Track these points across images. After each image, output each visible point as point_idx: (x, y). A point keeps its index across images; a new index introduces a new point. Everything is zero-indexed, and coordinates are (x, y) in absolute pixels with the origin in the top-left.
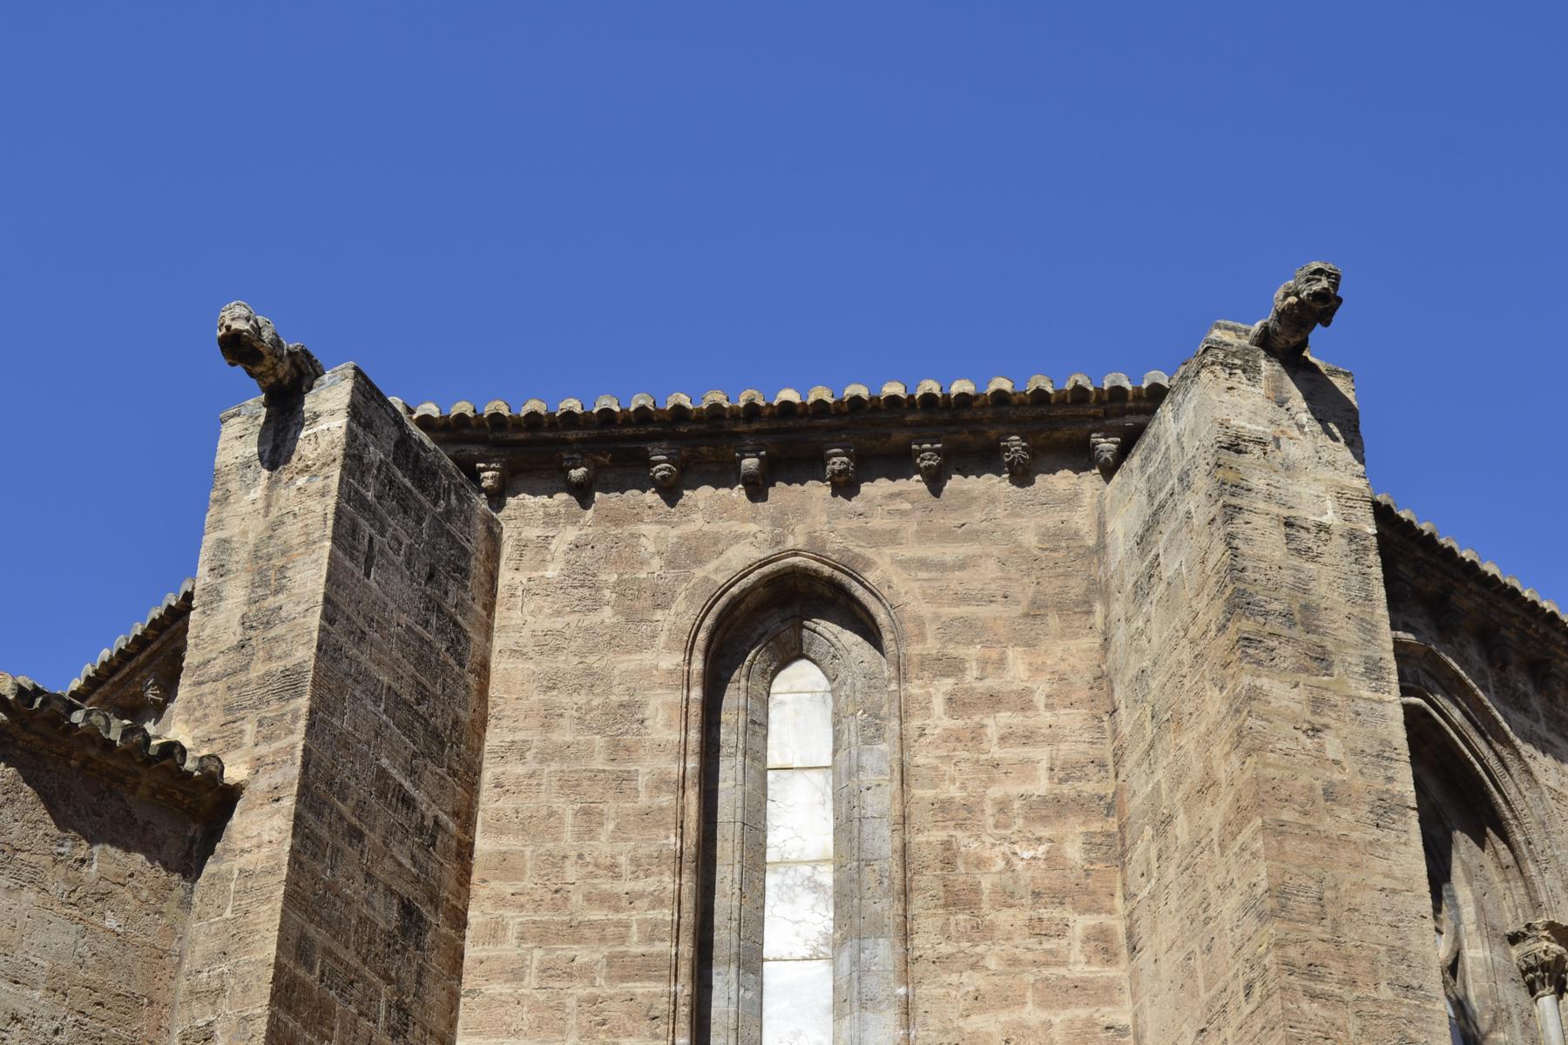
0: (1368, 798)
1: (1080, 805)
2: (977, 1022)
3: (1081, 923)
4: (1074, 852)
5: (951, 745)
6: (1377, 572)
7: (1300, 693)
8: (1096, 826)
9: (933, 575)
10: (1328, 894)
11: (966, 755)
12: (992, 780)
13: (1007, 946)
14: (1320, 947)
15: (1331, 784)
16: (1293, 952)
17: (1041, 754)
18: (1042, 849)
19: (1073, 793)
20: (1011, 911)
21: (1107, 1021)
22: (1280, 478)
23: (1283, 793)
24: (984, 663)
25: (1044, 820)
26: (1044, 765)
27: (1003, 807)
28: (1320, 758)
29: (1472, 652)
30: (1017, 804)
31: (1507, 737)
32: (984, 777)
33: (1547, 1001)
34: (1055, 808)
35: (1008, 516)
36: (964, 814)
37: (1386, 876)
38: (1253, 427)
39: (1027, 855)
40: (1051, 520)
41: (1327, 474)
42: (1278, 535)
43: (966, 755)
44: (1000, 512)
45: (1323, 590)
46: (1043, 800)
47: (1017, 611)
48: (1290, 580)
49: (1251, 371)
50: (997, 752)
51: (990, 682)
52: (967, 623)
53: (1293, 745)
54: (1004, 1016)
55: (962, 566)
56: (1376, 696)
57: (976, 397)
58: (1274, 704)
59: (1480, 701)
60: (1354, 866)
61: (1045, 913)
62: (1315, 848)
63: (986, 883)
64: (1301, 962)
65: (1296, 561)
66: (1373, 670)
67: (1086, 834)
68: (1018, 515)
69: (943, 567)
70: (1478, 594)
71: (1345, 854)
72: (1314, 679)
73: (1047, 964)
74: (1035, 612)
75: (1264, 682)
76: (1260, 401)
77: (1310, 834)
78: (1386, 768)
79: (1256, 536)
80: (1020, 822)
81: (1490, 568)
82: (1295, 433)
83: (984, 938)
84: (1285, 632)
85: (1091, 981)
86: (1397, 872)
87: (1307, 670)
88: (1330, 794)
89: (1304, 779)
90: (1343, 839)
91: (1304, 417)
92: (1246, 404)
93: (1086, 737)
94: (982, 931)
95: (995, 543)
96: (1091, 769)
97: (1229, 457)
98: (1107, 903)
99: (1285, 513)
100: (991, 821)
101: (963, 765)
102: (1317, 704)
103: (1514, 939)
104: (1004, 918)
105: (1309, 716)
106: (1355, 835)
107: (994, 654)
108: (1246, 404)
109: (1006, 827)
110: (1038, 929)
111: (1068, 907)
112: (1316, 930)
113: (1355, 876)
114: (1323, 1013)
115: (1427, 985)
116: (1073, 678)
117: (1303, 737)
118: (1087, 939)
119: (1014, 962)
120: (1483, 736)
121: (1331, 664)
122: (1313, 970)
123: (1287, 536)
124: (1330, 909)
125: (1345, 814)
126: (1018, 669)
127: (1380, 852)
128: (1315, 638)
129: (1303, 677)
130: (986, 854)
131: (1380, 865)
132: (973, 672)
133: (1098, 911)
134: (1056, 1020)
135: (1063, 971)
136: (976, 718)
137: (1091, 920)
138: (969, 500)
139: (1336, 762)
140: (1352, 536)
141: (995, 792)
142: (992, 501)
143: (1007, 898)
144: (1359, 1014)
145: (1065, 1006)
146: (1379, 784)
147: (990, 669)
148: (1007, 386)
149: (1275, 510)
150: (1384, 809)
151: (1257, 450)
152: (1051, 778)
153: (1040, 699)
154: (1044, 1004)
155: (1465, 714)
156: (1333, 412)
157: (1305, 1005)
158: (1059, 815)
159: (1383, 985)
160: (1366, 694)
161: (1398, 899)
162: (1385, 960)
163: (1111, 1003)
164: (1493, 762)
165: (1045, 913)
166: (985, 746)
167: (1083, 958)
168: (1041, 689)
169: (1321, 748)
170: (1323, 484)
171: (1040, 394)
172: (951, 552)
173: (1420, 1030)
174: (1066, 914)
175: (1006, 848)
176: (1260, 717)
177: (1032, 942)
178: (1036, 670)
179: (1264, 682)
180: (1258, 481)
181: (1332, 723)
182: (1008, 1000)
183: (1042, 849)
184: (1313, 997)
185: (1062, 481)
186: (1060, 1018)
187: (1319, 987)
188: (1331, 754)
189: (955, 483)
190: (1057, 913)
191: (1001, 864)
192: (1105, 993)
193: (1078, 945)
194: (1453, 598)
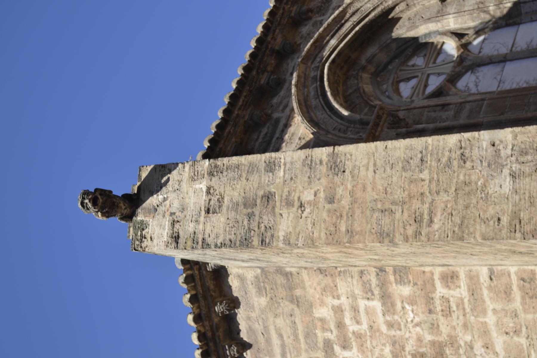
0: (331, 176)
1: (383, 285)
2: (499, 347)
3: (440, 290)
4: (406, 290)
5: (365, 350)
6: (226, 160)
7: (284, 212)
8: (392, 278)
9: (287, 351)
10: (379, 206)
11: (369, 342)
12: (379, 330)
13: (459, 329)
14: (406, 214)
15: (326, 198)
16: (410, 231)
17: (362, 304)
18: (408, 307)
19: (378, 289)
20: (441, 326)
21: (488, 279)
22: (189, 213)
23: (332, 229)
24: (324, 329)
25: (393, 305)
26: (366, 302)
27: (390, 325)
28: (314, 204)
29: (304, 30)
30: (388, 318)
31: (342, 12)
32: (378, 334)
34: (386, 298)
35: (255, 311)
36: (397, 346)
37: (367, 169)
38: (167, 227)
39: (412, 315)
40: (252, 290)
41: (184, 185)
42: (214, 218)
43: (369, 342)
44: (253, 315)
45: (236, 194)
46: (384, 304)
47: (297, 311)
48: (233, 213)
49: (143, 226)
50: (364, 327)
51: (332, 326)
52: (307, 336)
53: (309, 220)
54: (494, 334)
55: (281, 336)
56: (283, 167)
57: (199, 332)
58: (291, 229)
59: (325, 29)
60: (364, 189)
61: (439, 308)
62: (358, 212)
63: (428, 338)
64: (414, 227)
65: (224, 208)
66: (271, 167)
67: (396, 283)
68: (253, 306)
69: (283, 346)
70: (274, 34)
71: (359, 194)
72: (278, 204)
73: (464, 309)
74: (296, 301)
75: (281, 234)
76: (155, 223)
77: (351, 216)
78: (316, 164)
79: (215, 231)
80: (396, 317)
81: (260, 29)
82: (167, 202)
83: (456, 341)
84: (257, 218)
85: (469, 287)
86: (365, 162)
87: (274, 208)
88: (331, 200)
89: (325, 215)
90: (352, 193)
91: (161, 197)
92: (157, 231)
93: (349, 279)
94: (453, 341)
95: (267, 318)
96: (364, 278)
97: (181, 241)
98: (428, 275)
99: (203, 213)
100: (398, 332)
101: (374, 344)
102: (289, 203)
104: (445, 329)
105: (295, 209)
106: (349, 187)
107: (319, 324)
108: (157, 231)
109: (399, 324)
110: (448, 312)
111: (434, 295)
112: (398, 215)
113: (369, 189)
114: (439, 214)
115: (420, 149)
116: (323, 285)
117: (305, 214)
118: (448, 287)
119: (465, 326)
120: (342, 25)
121: (270, 192)
122: (418, 220)
123: (213, 213)
124: (387, 206)
125: (340, 191)
126: (323, 312)
127: (356, 171)
128: (258, 201)
129: (277, 210)
130: (415, 336)
131: (363, 173)
132: (328, 335)
133: (433, 280)
134: (492, 307)
135: (466, 301)
136: (351, 335)
137: (438, 284)
138: (250, 329)
139: (315, 195)
140: (211, 174)
141: (384, 328)
142: (249, 318)
143: (434, 327)
144: (438, 193)
145: (484, 301)
146: (324, 169)
147: (326, 327)
148: (190, 317)
149: (202, 219)
150: (336, 167)
151: (177, 226)
152: (373, 300)
153: (336, 302)
154: (484, 312)
155: (332, 37)
156: (154, 183)
157: (436, 226)
158: (389, 297)
159: (422, 176)
160: (282, 173)
161: (379, 163)
162: (409, 174)
163: (478, 276)
164: (355, 18)
165: (439, 308)
166: (363, 332)
167: (458, 290)
168: (331, 301)
169: (309, 202)
170: (187, 190)
171: (191, 300)
172: (276, 341)
173: (443, 155)
174: (437, 297)
175: (410, 325)
176: (297, 239)
177: (455, 316)
178: (323, 303)
179: (281, 234)
180: (191, 228)
181: (297, 195)
182: (485, 332)
183: (408, 307)
184: (431, 221)
185: (234, 282)
186: (490, 305)
187: (426, 217)
188: (311, 198)
189: (244, 335)
190: (438, 302)
191: (418, 329)
192: (473, 278)
193: (452, 292)
194: (277, 48)
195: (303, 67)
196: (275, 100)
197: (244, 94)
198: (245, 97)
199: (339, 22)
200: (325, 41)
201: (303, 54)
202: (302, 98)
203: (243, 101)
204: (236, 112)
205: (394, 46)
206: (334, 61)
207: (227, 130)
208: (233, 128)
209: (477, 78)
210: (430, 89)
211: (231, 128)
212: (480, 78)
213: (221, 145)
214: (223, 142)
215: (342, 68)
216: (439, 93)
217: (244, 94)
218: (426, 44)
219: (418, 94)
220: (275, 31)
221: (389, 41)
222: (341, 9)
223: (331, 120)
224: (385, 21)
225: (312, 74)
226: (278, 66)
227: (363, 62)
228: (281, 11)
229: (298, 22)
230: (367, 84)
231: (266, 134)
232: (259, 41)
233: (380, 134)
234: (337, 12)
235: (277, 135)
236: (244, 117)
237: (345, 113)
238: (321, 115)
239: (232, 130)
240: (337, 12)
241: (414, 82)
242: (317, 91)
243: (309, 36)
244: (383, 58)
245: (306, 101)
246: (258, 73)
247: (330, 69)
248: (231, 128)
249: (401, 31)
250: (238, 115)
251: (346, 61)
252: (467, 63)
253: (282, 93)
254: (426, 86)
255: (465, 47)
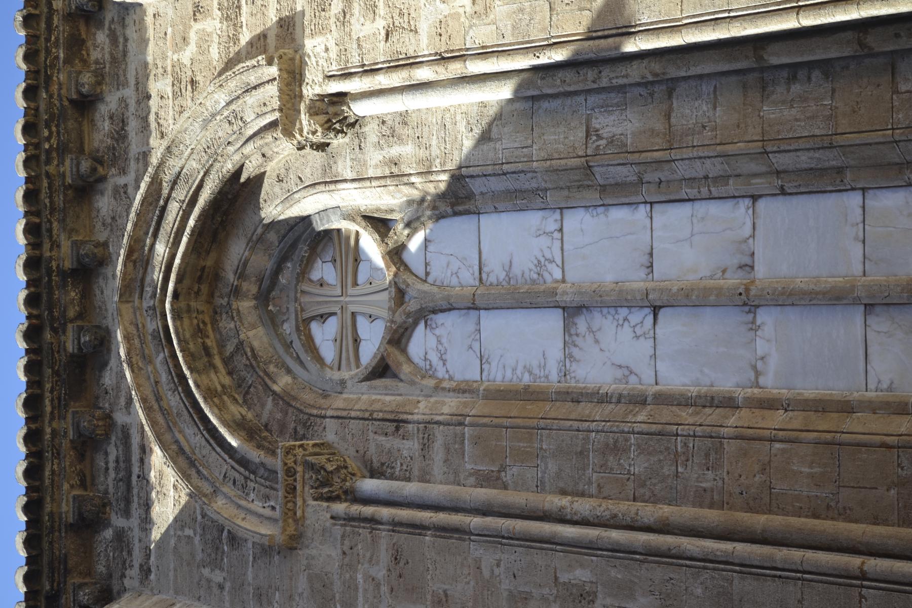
29: (104, 203)
33: (359, 109)
59: (135, 225)
70: (51, 237)
103: (322, 147)
120: (164, 209)
155: (155, 235)
164: (182, 193)
194: (68, 265)
195: (126, 309)
196: (108, 379)
197: (48, 386)
198: (52, 392)
199: (156, 203)
200: (146, 248)
201: (118, 282)
202: (148, 392)
203: (52, 401)
204: (48, 430)
205: (272, 237)
206: (176, 295)
207: (47, 473)
208: (56, 461)
209: (439, 342)
210: (369, 350)
211: (53, 464)
212: (444, 341)
213: (48, 508)
214: (48, 499)
215: (197, 293)
216: (382, 370)
217: (48, 386)
218: (328, 232)
219: (348, 359)
220: (50, 230)
221: (260, 230)
222: (147, 179)
223: (214, 453)
224: (238, 194)
225: (152, 325)
226: (87, 294)
227: (231, 277)
228: (45, 183)
229: (85, 190)
230: (253, 327)
231: (117, 461)
232: (31, 265)
233: (303, 512)
234: (143, 186)
235: (136, 470)
236: (65, 433)
237: (234, 443)
238: (193, 437)
239: (55, 467)
240: (143, 186)
241: (332, 325)
242: (171, 373)
243: (115, 224)
244: (262, 262)
245: (158, 399)
246: (55, 330)
247: (177, 316)
248: (53, 464)
249: (273, 210)
250: (54, 433)
251: (202, 275)
252: (412, 306)
253: (113, 363)
254: (356, 341)
255: (396, 254)
